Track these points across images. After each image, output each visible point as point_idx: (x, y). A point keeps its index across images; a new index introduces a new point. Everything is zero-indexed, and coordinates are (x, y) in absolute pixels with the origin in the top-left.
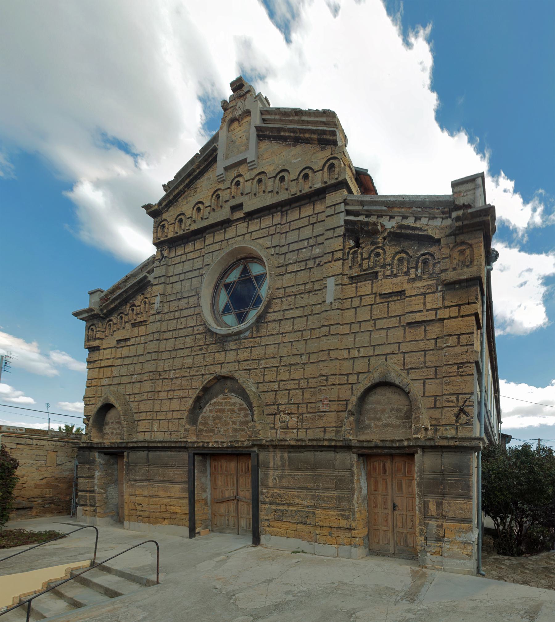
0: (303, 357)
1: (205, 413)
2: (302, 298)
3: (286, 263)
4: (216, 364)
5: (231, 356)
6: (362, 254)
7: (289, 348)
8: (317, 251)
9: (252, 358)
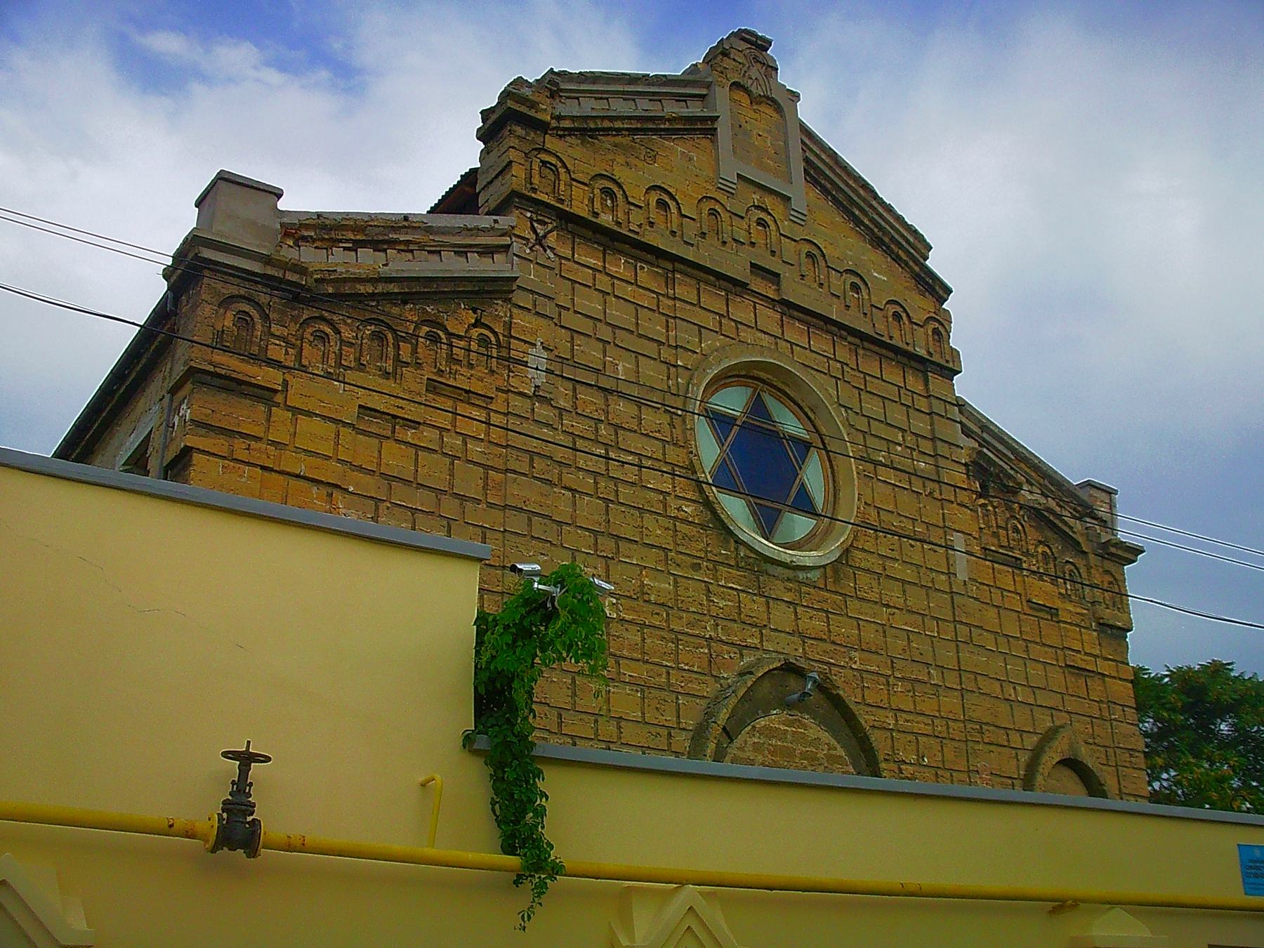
1: (741, 749)
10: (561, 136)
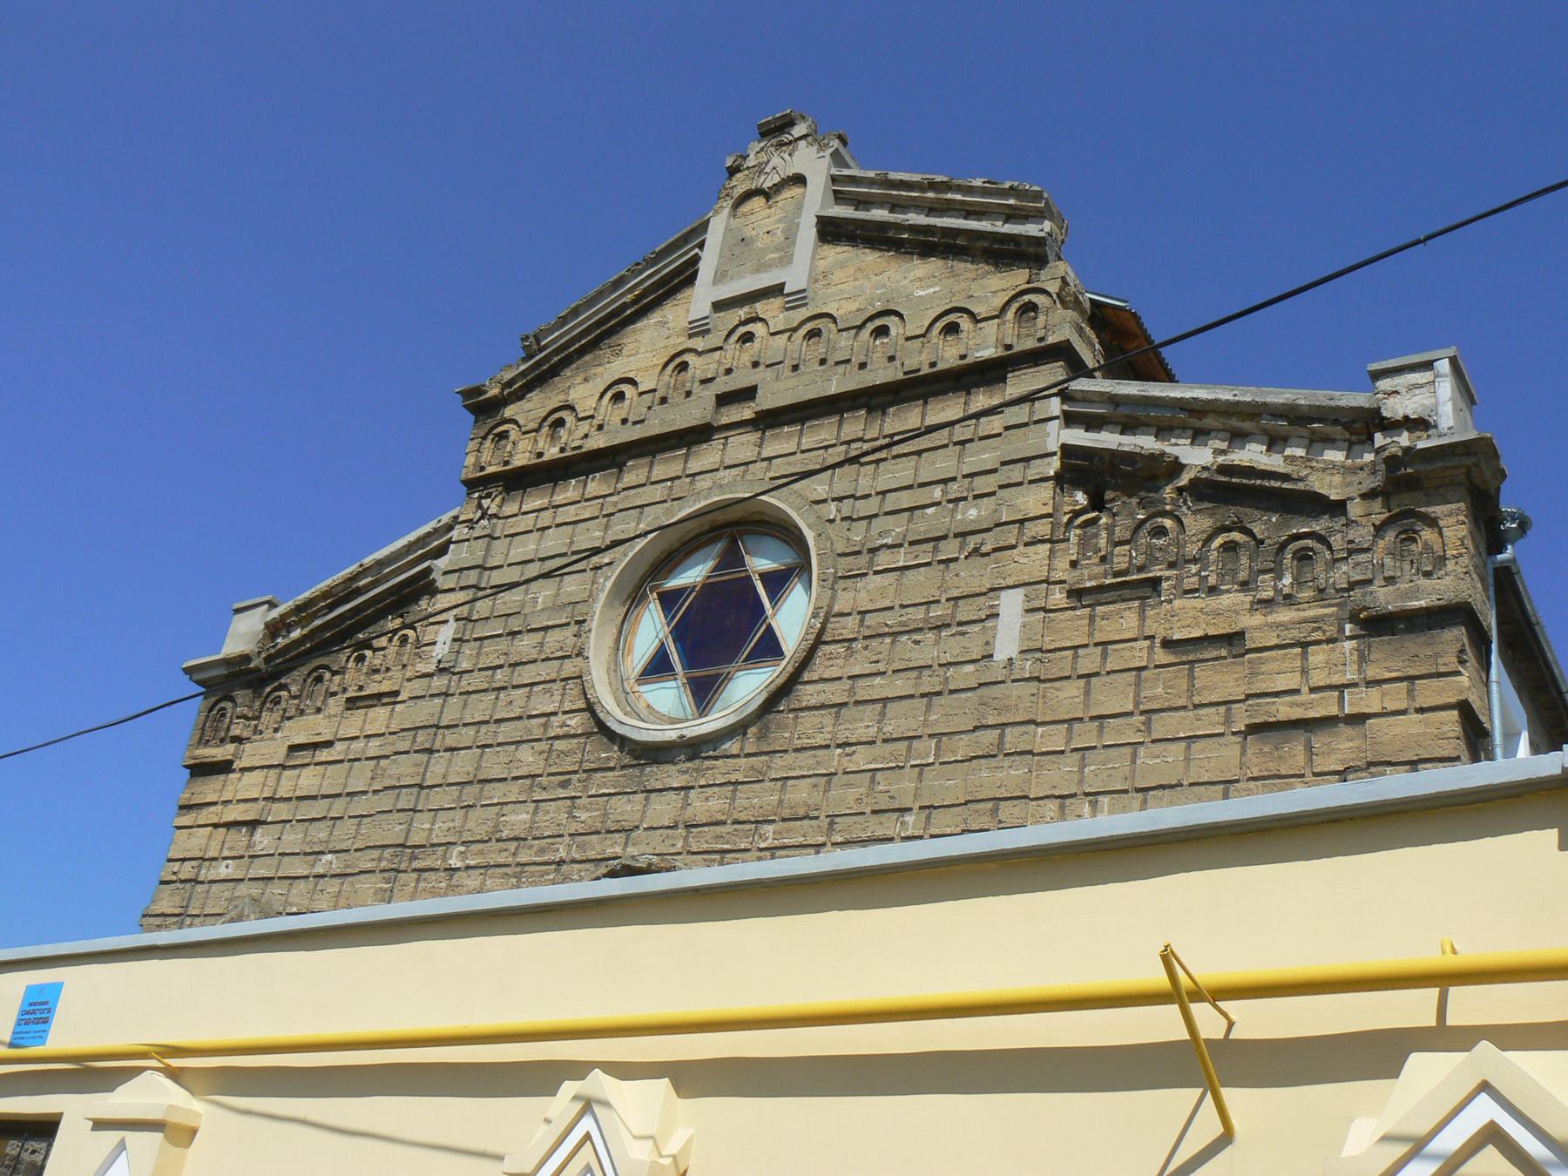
0: (909, 818)
2: (917, 642)
3: (870, 545)
4: (609, 832)
5: (664, 809)
6: (1110, 529)
7: (862, 790)
8: (972, 513)
9: (736, 816)
10: (521, 398)
